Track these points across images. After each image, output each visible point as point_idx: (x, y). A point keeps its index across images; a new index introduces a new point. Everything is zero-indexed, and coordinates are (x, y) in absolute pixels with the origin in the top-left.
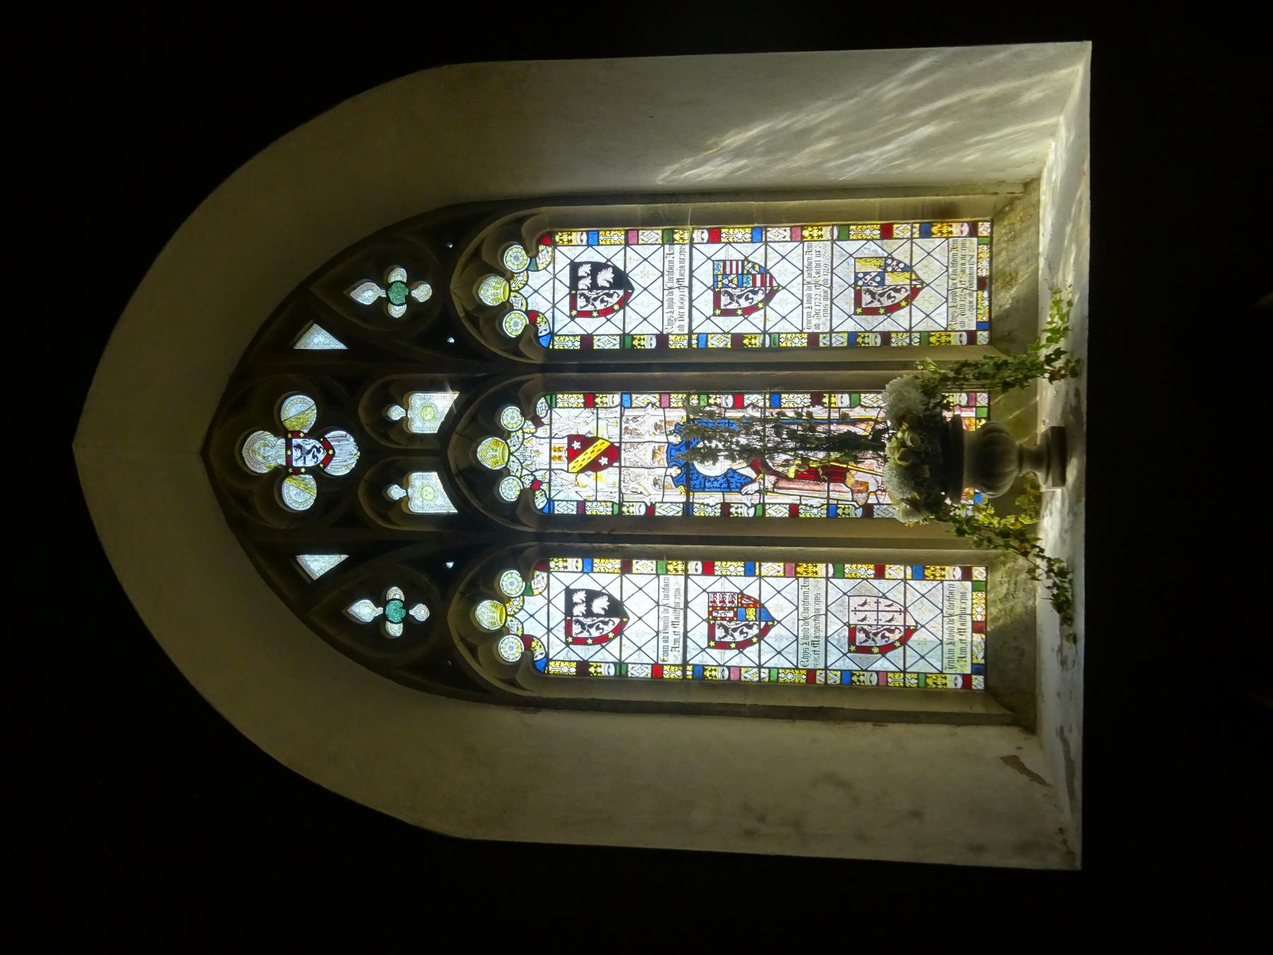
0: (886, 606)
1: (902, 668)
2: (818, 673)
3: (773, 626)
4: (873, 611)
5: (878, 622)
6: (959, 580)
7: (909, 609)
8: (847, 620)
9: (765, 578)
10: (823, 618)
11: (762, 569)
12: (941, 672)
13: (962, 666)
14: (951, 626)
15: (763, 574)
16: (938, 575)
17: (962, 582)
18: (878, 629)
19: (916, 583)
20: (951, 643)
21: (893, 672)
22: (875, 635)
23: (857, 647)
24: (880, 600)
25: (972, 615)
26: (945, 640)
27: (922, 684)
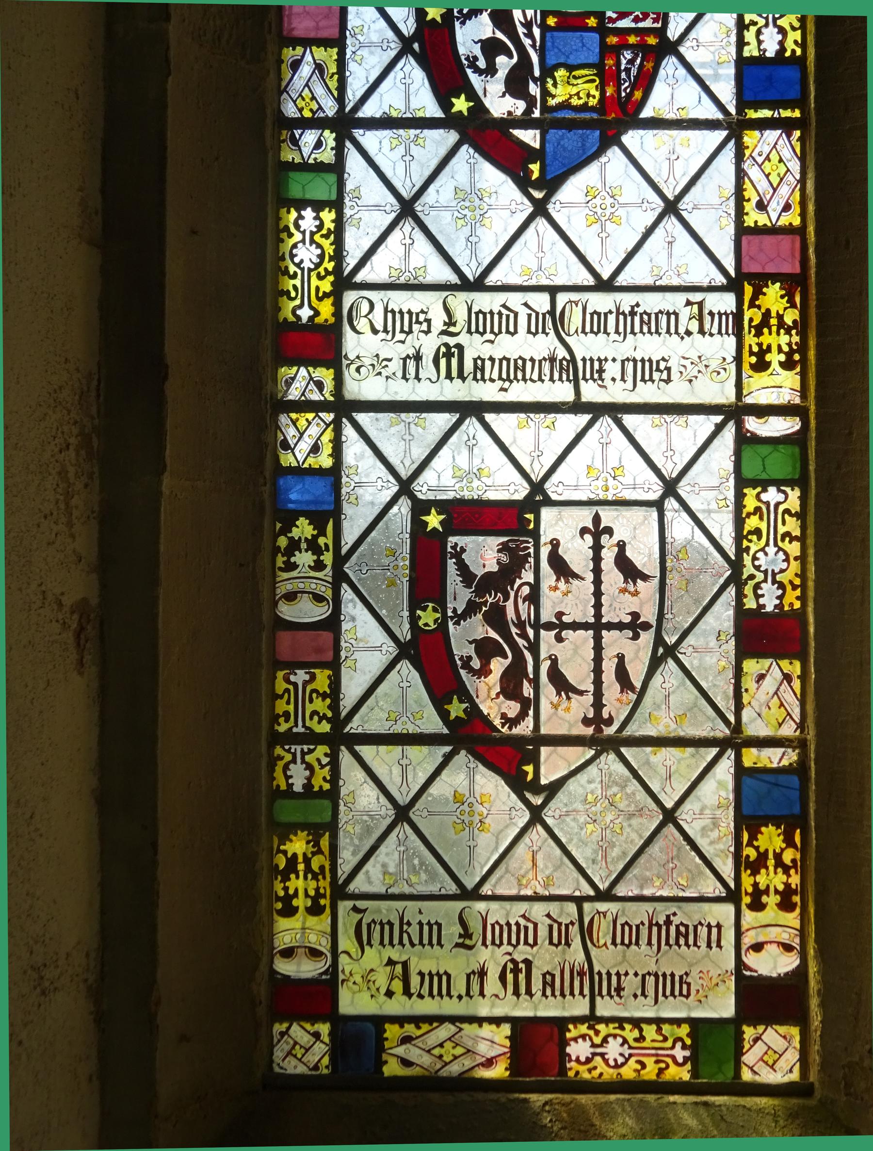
0: (621, 658)
1: (355, 726)
2: (326, 375)
3: (523, 183)
4: (598, 606)
5: (549, 626)
6: (740, 964)
7: (610, 760)
8: (554, 497)
9: (729, 151)
10: (563, 392)
11: (772, 135)
12: (340, 892)
13: (368, 975)
14: (543, 932)
15: (750, 138)
16: (762, 879)
17: (732, 984)
18: (521, 625)
19: (721, 784)
20: (467, 934)
21: (335, 692)
22: (496, 618)
23: (439, 538)
24: (647, 638)
25: (592, 1019)
26: (481, 906)
27: (287, 812)
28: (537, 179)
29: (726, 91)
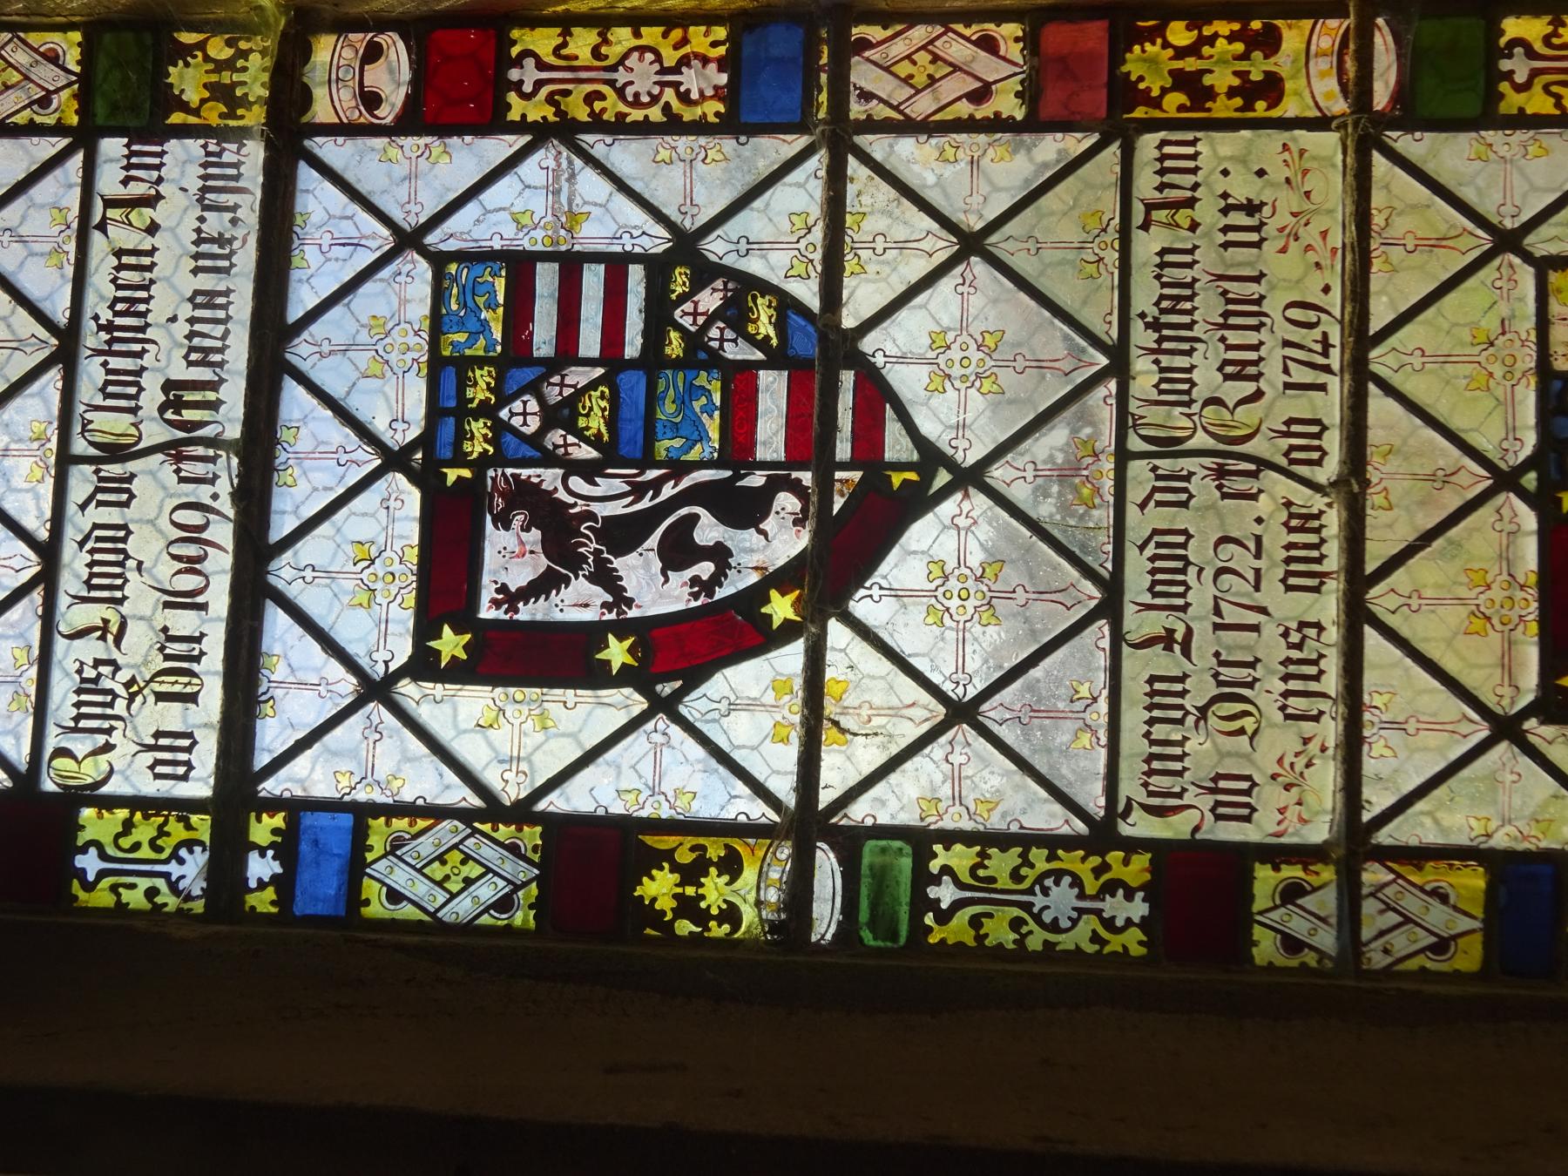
28: (919, 475)
29: (776, 148)
